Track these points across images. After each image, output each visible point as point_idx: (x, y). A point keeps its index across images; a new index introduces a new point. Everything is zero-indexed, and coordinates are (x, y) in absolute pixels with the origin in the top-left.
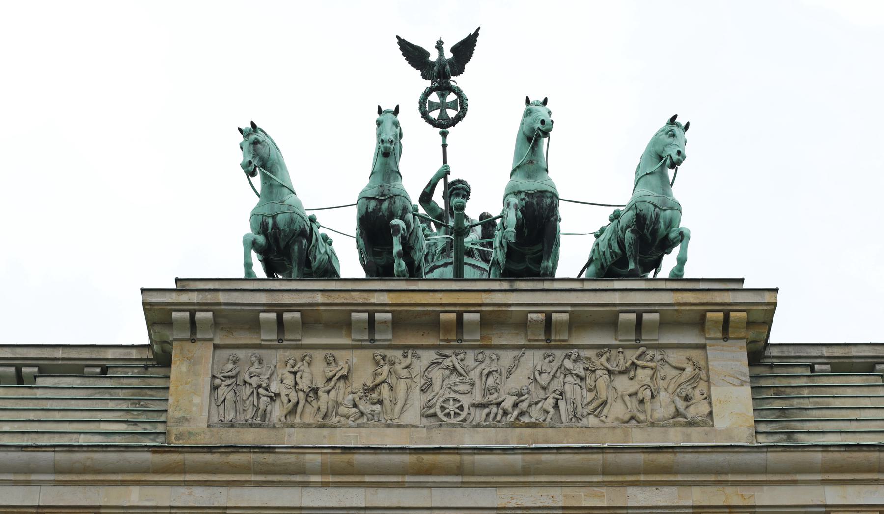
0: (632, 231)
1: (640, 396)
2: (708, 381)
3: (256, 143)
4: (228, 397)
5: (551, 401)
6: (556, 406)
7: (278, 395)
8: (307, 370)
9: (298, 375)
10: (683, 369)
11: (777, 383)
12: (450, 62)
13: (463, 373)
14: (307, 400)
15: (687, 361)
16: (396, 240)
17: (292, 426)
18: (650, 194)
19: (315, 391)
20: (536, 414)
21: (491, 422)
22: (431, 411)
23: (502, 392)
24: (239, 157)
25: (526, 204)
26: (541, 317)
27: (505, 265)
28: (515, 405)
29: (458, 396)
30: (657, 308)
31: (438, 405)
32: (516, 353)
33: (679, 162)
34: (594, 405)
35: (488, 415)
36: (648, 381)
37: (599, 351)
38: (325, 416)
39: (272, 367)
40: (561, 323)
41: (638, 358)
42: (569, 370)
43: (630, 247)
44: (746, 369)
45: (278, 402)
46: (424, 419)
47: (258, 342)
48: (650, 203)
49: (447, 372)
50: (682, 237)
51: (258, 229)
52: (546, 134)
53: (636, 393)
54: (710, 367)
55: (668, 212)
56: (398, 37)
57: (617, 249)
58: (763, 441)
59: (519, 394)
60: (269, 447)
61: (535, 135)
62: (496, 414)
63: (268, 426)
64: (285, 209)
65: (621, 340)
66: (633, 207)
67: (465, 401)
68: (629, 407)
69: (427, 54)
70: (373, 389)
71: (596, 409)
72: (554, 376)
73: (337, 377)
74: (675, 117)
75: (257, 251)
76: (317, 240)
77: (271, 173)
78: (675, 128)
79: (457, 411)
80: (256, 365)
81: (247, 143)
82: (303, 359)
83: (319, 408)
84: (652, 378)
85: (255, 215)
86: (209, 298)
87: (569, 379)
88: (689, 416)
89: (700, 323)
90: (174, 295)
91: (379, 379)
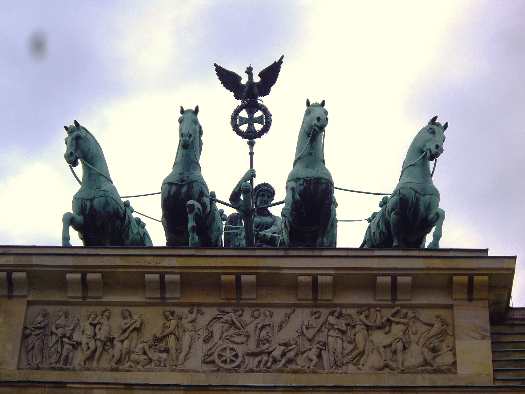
1: (393, 346)
2: (454, 335)
3: (78, 138)
4: (36, 344)
6: (319, 356)
7: (79, 344)
9: (98, 327)
10: (432, 325)
11: (516, 339)
12: (258, 84)
13: (241, 327)
14: (104, 348)
15: (436, 318)
16: (190, 217)
17: (88, 369)
19: (111, 340)
20: (301, 361)
22: (211, 359)
25: (305, 187)
26: (308, 279)
27: (288, 243)
28: (284, 354)
30: (409, 272)
32: (288, 311)
34: (354, 354)
35: (260, 362)
38: (119, 362)
39: (76, 321)
40: (325, 285)
41: (394, 315)
42: (332, 325)
43: (394, 226)
45: (79, 349)
47: (66, 299)
48: (411, 189)
49: (227, 326)
53: (390, 345)
54: (456, 323)
55: (427, 197)
56: (215, 65)
57: (384, 230)
58: (498, 384)
60: (62, 383)
61: (314, 131)
62: (267, 362)
63: (68, 369)
64: (102, 193)
65: (378, 300)
66: (398, 192)
67: (241, 350)
68: (384, 357)
69: (240, 78)
70: (161, 340)
72: (319, 331)
73: (131, 329)
74: (435, 118)
75: (76, 228)
76: (130, 222)
77: (92, 164)
78: (435, 127)
79: (233, 358)
80: (63, 318)
81: (70, 138)
82: (102, 315)
83: (114, 355)
84: (404, 333)
86: (23, 261)
87: (332, 332)
88: (435, 365)
89: (448, 286)
91: (167, 331)
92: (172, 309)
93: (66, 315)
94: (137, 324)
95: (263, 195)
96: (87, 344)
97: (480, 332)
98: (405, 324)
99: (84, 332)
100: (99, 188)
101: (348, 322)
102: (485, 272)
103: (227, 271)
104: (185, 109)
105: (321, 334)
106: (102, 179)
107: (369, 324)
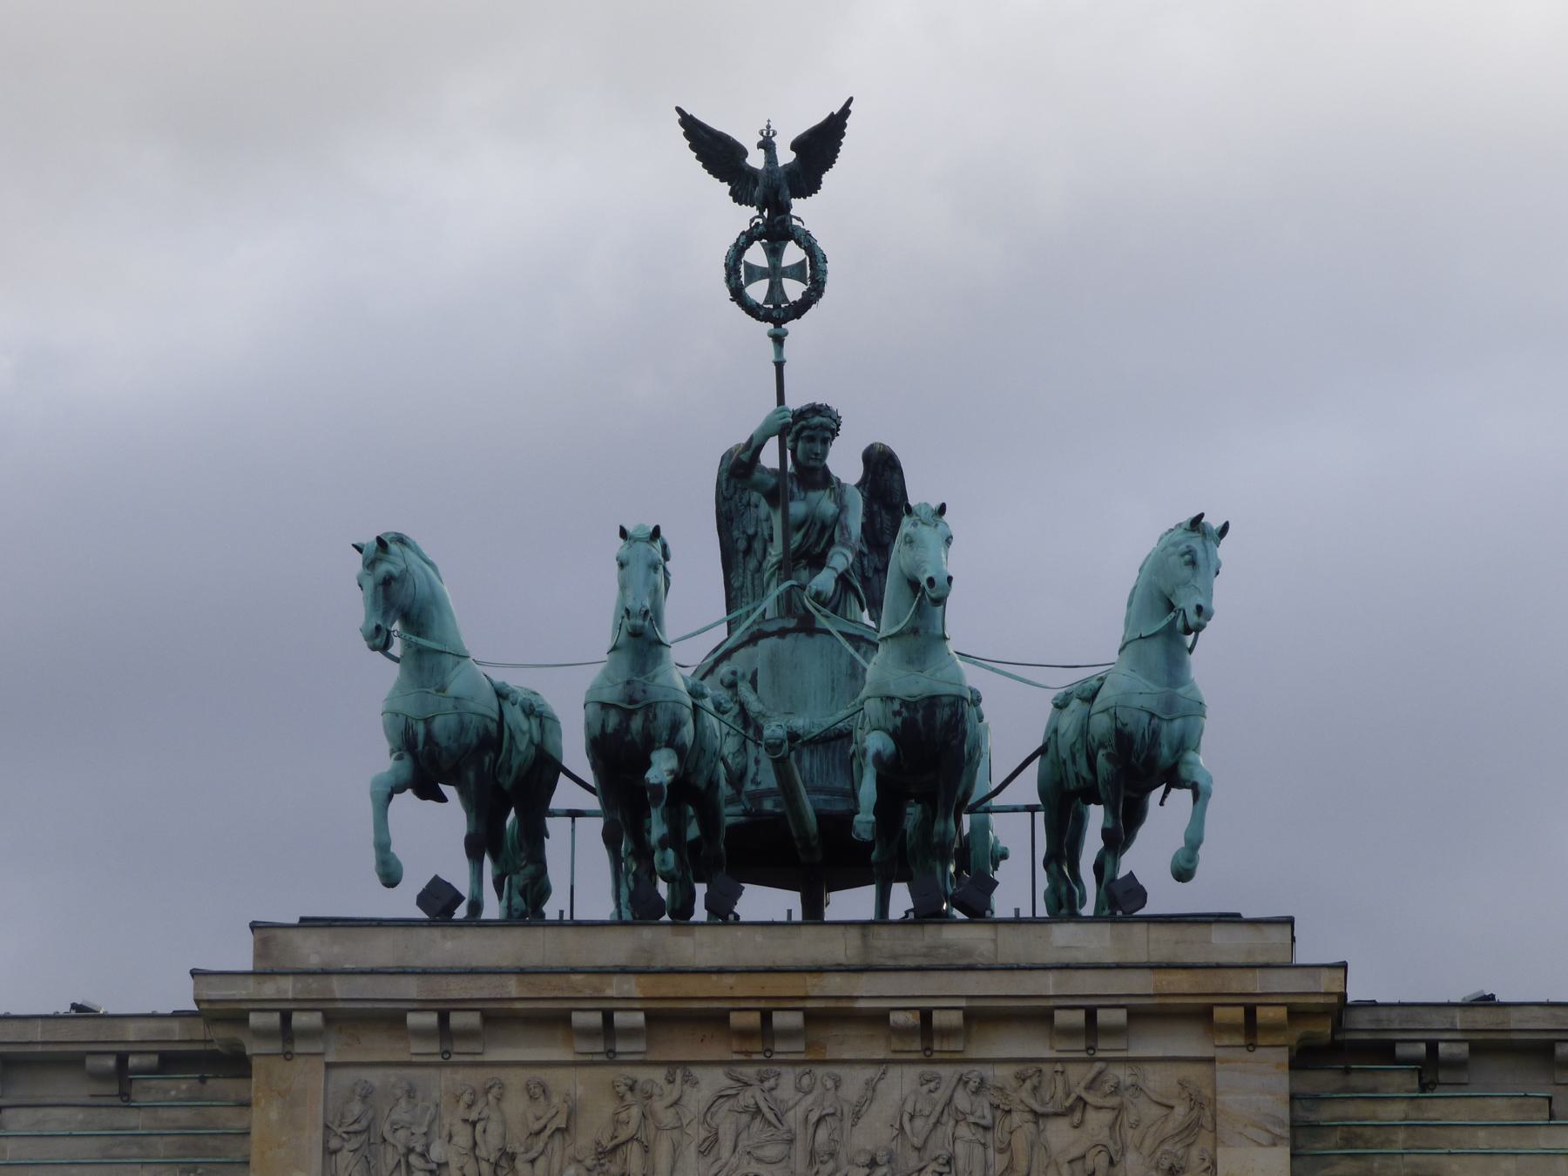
0: (1109, 757)
1: (1089, 1164)
9: (479, 1127)
10: (1172, 1108)
19: (512, 1157)
23: (843, 1157)
26: (912, 1019)
30: (1123, 1001)
32: (870, 1072)
33: (1199, 628)
36: (1104, 1136)
39: (432, 1109)
40: (948, 1033)
44: (1284, 1112)
47: (404, 1057)
48: (1141, 709)
49: (745, 1118)
50: (1199, 794)
52: (940, 601)
55: (1178, 723)
56: (679, 110)
57: (1085, 772)
69: (745, 153)
72: (938, 1122)
73: (548, 1132)
74: (1202, 516)
76: (512, 737)
77: (418, 635)
78: (1196, 542)
80: (403, 1103)
81: (369, 583)
82: (487, 1092)
84: (1112, 1127)
85: (393, 714)
86: (315, 987)
87: (964, 1131)
90: (251, 981)
91: (622, 1137)
93: (411, 1093)
94: (560, 1122)
95: (811, 439)
96: (461, 1168)
97: (1269, 1127)
98: (1113, 1109)
99: (450, 1137)
100: (442, 689)
101: (996, 1102)
102: (1280, 1000)
103: (743, 1005)
104: (630, 529)
105: (940, 1130)
106: (448, 661)
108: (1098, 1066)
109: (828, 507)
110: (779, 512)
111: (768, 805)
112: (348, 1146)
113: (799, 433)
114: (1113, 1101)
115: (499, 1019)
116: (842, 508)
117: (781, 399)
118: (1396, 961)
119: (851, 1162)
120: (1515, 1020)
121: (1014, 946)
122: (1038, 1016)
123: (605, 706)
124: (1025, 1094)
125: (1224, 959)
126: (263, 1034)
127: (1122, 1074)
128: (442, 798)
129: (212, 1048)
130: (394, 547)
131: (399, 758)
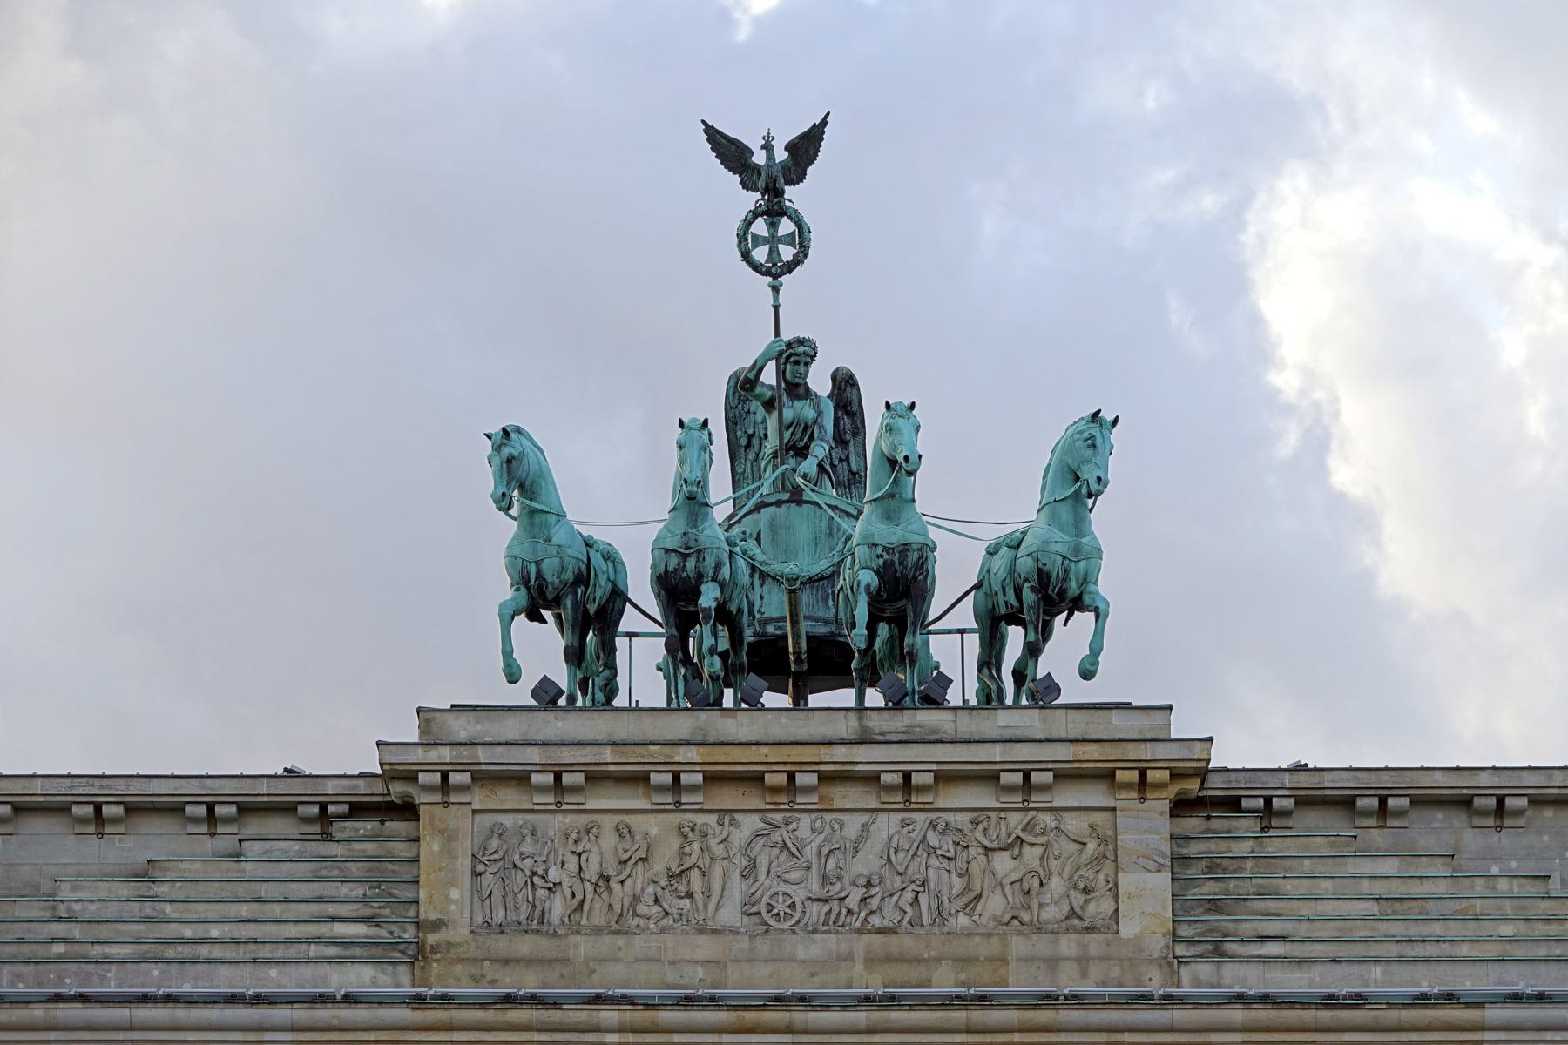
0: (1032, 589)
4: (495, 892)
5: (909, 895)
8: (595, 849)
9: (583, 857)
12: (784, 167)
17: (578, 933)
18: (1061, 542)
19: (607, 879)
21: (831, 925)
22: (755, 909)
23: (846, 881)
24: (486, 480)
26: (897, 779)
28: (863, 900)
29: (789, 889)
30: (1050, 766)
31: (765, 899)
32: (865, 818)
34: (965, 900)
35: (829, 912)
37: (975, 814)
40: (923, 789)
44: (1166, 847)
46: (746, 919)
48: (1056, 553)
49: (776, 851)
51: (517, 578)
55: (1082, 564)
59: (869, 884)
63: (547, 933)
67: (799, 894)
71: (967, 906)
80: (528, 839)
81: (497, 461)
82: (588, 832)
84: (1042, 858)
85: (512, 558)
86: (465, 754)
87: (933, 861)
89: (1107, 776)
90: (420, 750)
92: (689, 816)
95: (797, 363)
100: (548, 539)
103: (775, 768)
105: (917, 859)
106: (552, 519)
107: (989, 845)
108: (1032, 813)
109: (809, 413)
110: (775, 414)
111: (770, 629)
112: (490, 870)
113: (788, 358)
114: (1040, 840)
115: (596, 778)
116: (820, 414)
117: (777, 334)
118: (1253, 736)
119: (853, 883)
120: (1328, 781)
121: (968, 725)
122: (989, 777)
123: (667, 551)
124: (979, 834)
125: (1122, 736)
126: (429, 789)
127: (1048, 819)
128: (544, 621)
129: (390, 801)
130: (513, 436)
131: (518, 590)
